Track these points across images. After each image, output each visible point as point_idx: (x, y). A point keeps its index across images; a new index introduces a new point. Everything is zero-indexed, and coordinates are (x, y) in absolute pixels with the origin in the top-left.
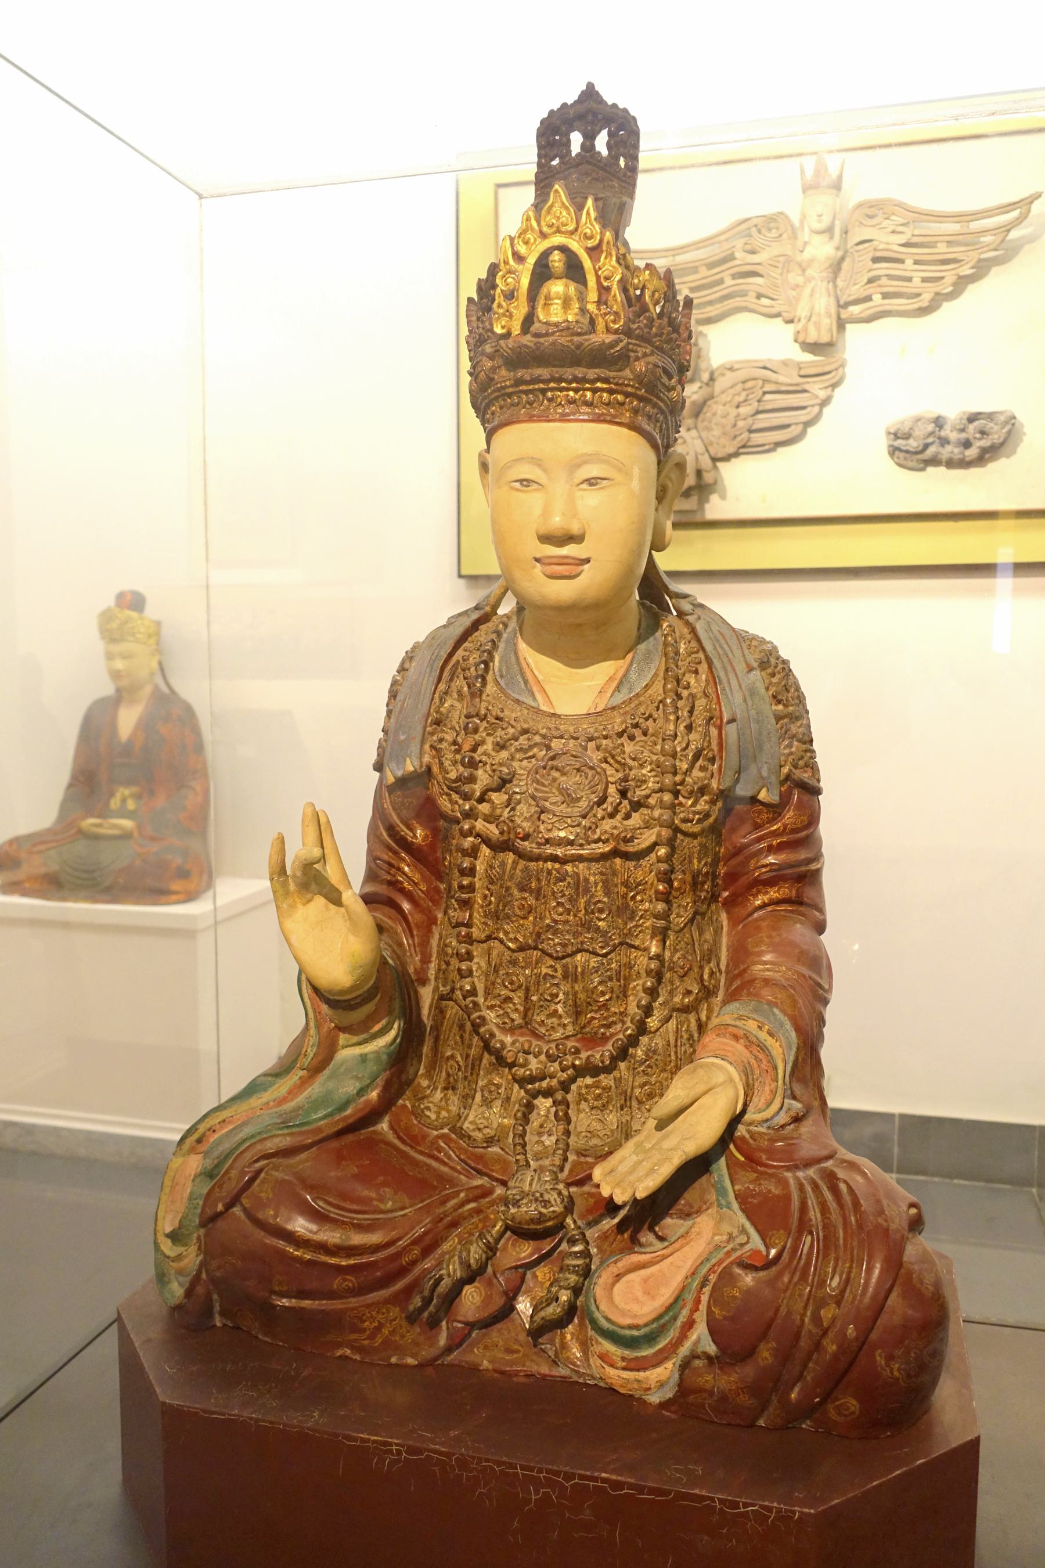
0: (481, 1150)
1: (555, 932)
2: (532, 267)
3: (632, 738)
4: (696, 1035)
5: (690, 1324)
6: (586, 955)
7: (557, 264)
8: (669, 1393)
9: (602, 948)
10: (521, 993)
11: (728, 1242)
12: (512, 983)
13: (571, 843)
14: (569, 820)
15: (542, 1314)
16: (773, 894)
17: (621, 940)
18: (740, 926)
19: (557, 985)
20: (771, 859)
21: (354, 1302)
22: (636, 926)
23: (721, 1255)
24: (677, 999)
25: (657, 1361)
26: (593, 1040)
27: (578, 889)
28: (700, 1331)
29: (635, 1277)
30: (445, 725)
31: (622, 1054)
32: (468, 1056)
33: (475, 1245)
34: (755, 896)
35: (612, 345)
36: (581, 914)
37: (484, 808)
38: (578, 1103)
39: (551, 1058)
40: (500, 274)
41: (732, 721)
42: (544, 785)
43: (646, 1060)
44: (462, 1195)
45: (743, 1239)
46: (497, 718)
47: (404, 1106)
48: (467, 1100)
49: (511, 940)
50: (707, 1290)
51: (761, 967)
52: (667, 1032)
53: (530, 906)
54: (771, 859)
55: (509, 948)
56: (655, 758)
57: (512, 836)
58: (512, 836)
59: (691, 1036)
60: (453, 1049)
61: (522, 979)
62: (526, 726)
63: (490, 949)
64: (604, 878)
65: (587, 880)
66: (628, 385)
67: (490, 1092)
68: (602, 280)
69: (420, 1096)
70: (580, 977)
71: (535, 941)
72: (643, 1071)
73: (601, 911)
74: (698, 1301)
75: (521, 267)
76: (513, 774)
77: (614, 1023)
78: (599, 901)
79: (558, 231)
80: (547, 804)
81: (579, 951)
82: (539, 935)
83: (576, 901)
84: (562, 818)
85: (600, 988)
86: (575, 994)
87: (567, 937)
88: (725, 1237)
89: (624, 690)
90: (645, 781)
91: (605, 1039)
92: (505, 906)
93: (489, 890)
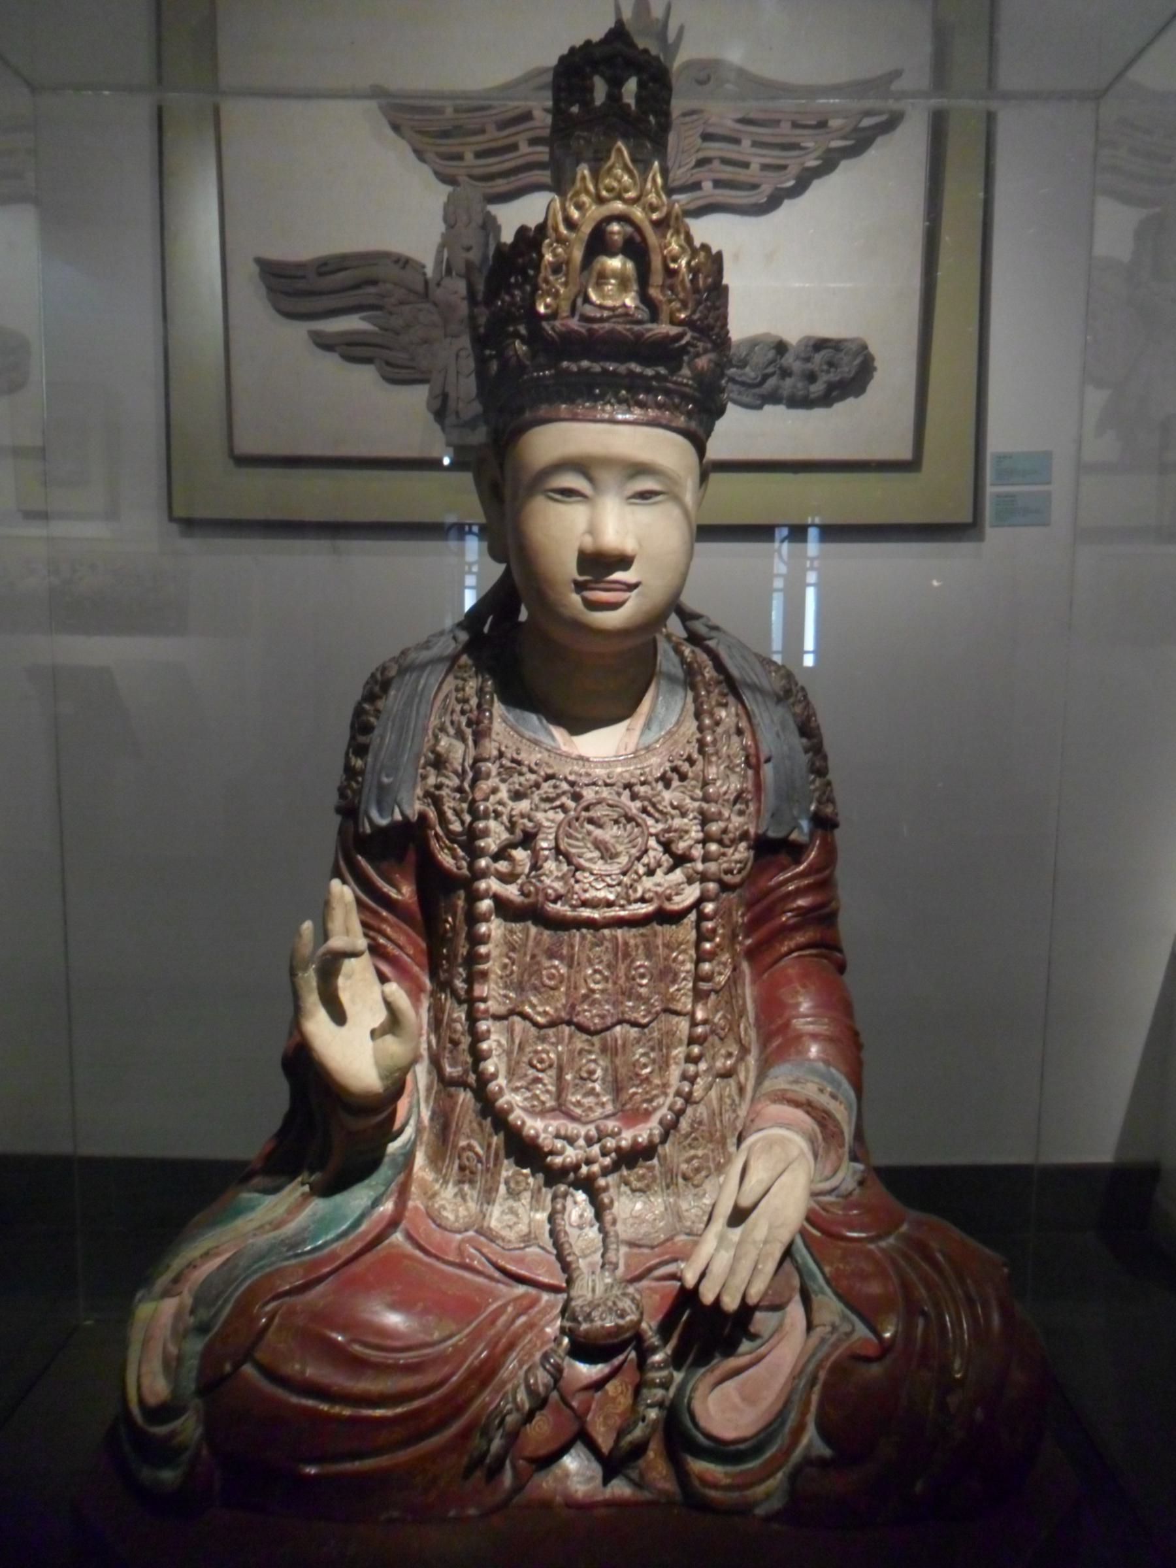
0: (517, 1252)
1: (593, 1003)
2: (586, 238)
3: (667, 785)
4: (737, 1099)
5: (800, 1429)
6: (627, 1027)
7: (616, 237)
8: (776, 1504)
9: (644, 1016)
10: (553, 1072)
11: (832, 1333)
12: (541, 1061)
13: (610, 904)
14: (608, 879)
15: (629, 1438)
16: (800, 939)
17: (663, 1006)
18: (766, 975)
19: (595, 1061)
20: (801, 902)
21: (403, 1455)
22: (678, 990)
23: (825, 1348)
24: (719, 1064)
25: (767, 1472)
26: (635, 1116)
27: (616, 955)
28: (810, 1434)
29: (730, 1385)
30: (446, 768)
31: (669, 1128)
32: (489, 1146)
33: (541, 1369)
34: (782, 944)
35: (680, 336)
36: (622, 981)
37: (503, 866)
38: (619, 1187)
39: (590, 1142)
40: (547, 241)
41: (768, 760)
42: (577, 839)
43: (691, 1133)
44: (510, 1309)
45: (846, 1328)
46: (513, 761)
47: (416, 1208)
48: (488, 1196)
49: (539, 1014)
50: (817, 1389)
51: (802, 1020)
52: (711, 1101)
53: (562, 975)
54: (801, 902)
55: (535, 1024)
56: (696, 804)
57: (541, 898)
58: (541, 898)
59: (733, 1101)
60: (468, 1137)
61: (552, 1055)
62: (550, 771)
63: (513, 1024)
64: (645, 939)
65: (626, 944)
66: (686, 385)
67: (518, 1183)
68: (669, 261)
69: (430, 1193)
70: (620, 1050)
71: (570, 1014)
72: (690, 1145)
73: (642, 976)
74: (807, 1403)
75: (573, 235)
76: (539, 826)
77: (656, 1096)
78: (641, 966)
79: (619, 197)
80: (582, 861)
81: (620, 1022)
82: (573, 1007)
83: (615, 967)
84: (600, 877)
85: (643, 1060)
86: (615, 1070)
87: (607, 1007)
88: (828, 1329)
89: (655, 727)
90: (687, 832)
91: (648, 1114)
92: (531, 976)
93: (510, 958)
